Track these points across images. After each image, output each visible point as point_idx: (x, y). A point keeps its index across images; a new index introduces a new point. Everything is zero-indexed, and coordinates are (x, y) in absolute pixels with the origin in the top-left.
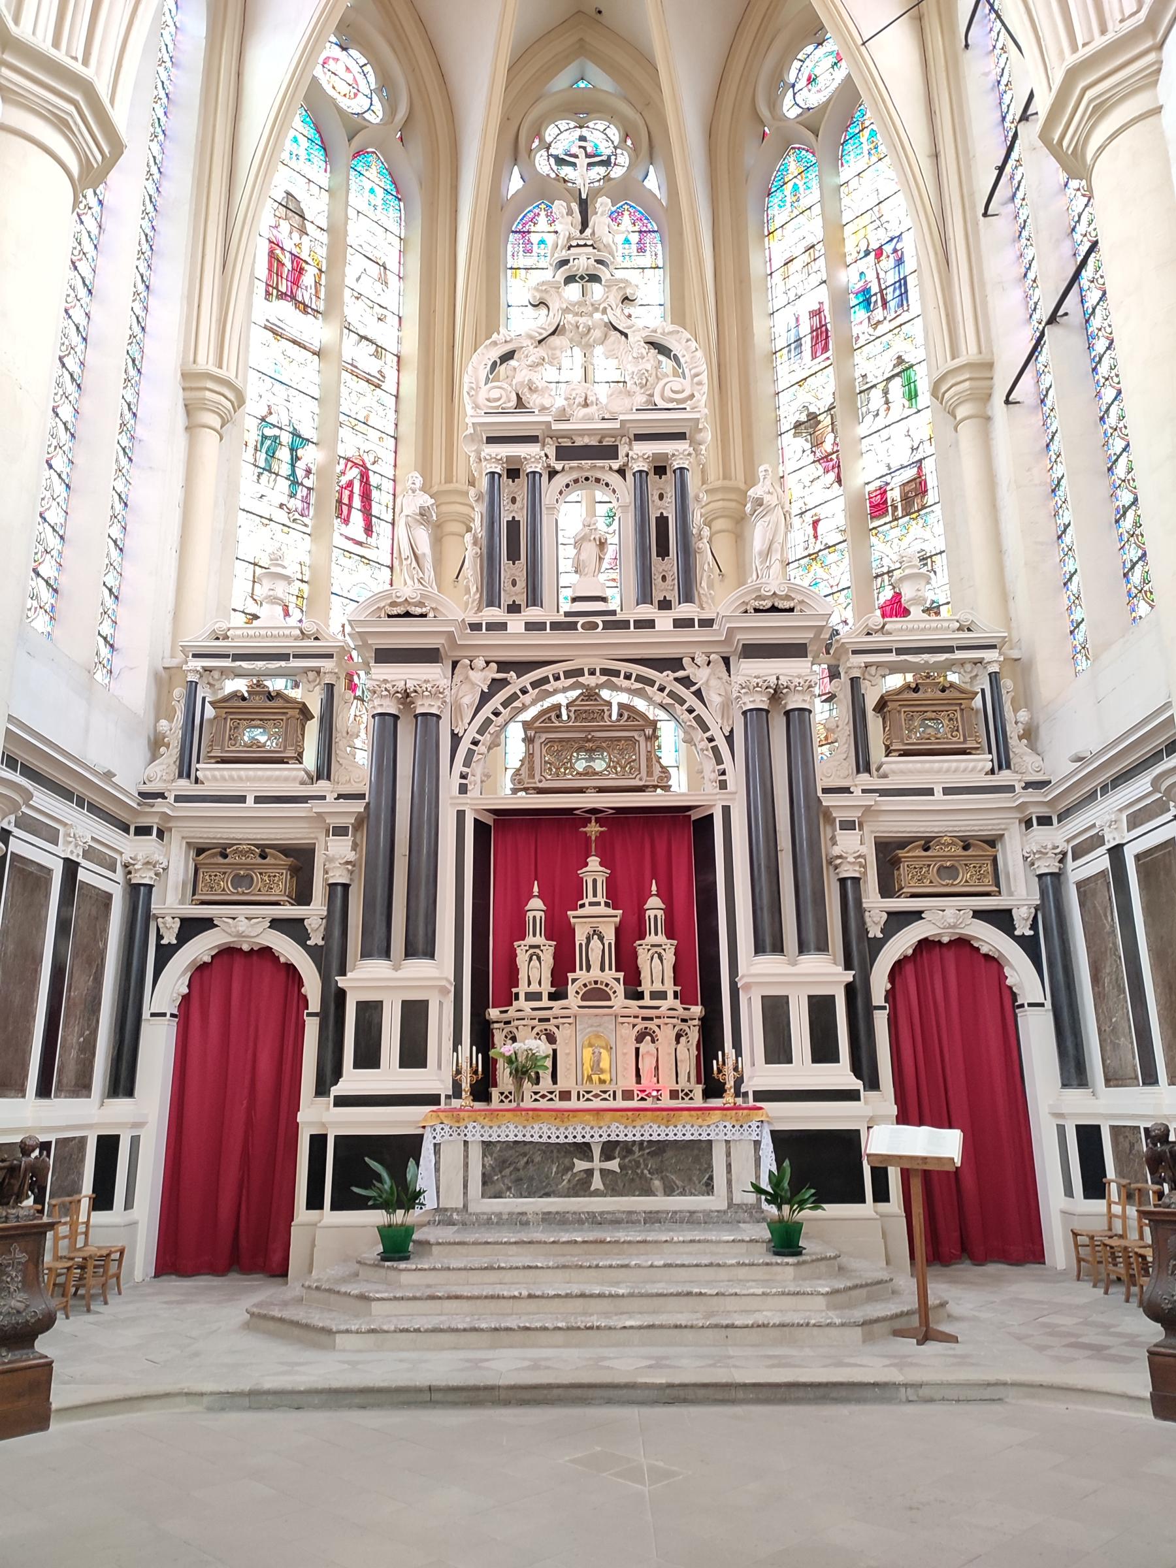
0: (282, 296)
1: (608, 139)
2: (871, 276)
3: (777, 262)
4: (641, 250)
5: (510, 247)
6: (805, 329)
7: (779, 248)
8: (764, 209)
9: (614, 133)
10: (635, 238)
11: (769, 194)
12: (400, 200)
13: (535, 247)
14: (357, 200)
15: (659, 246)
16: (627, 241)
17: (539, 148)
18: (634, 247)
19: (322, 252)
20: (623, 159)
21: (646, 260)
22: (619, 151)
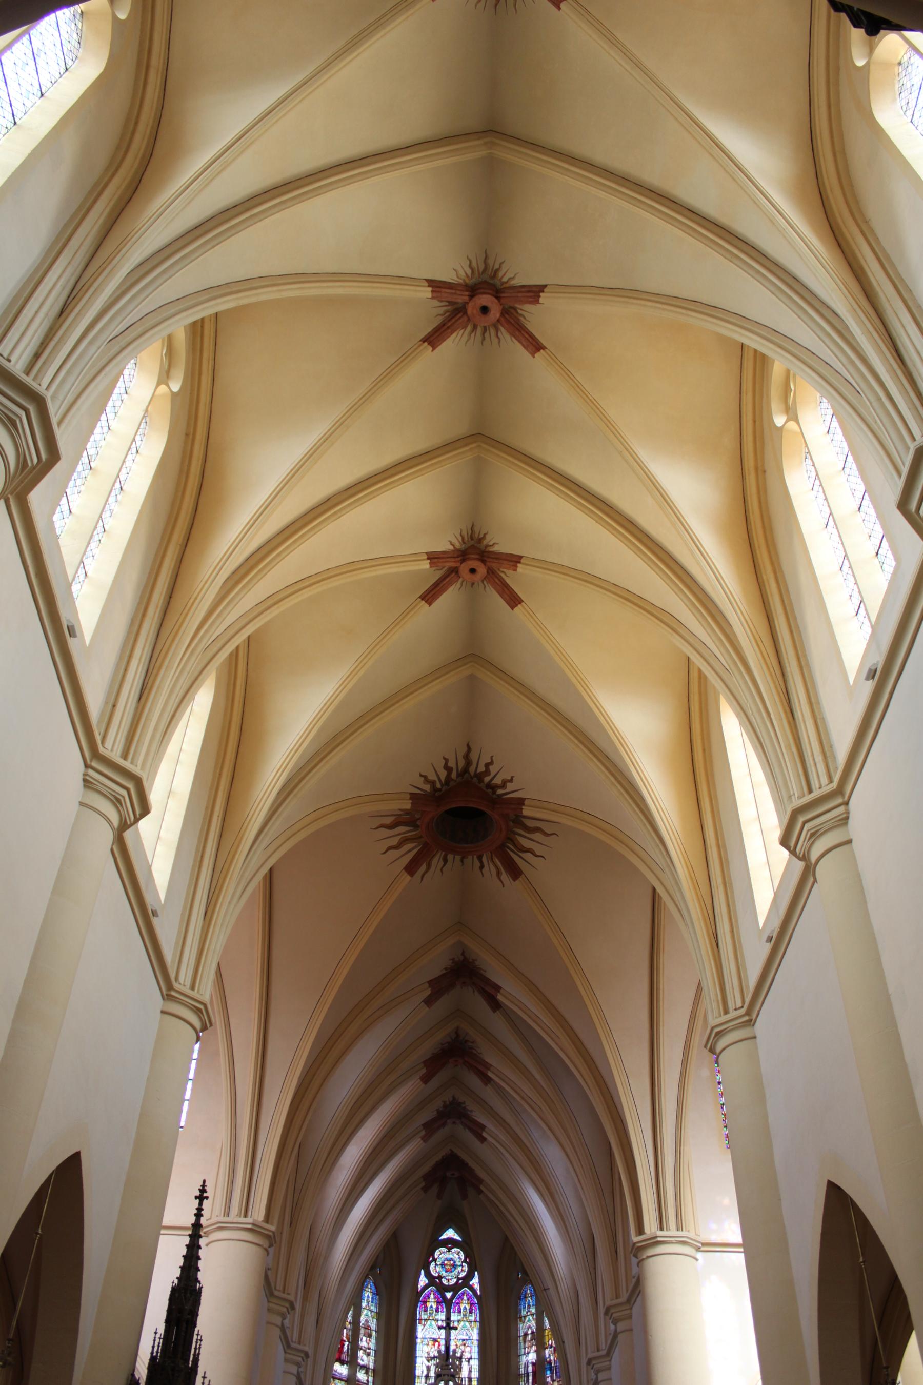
0: (337, 1361)
1: (460, 1258)
2: (552, 1358)
3: (522, 1334)
4: (471, 1312)
5: (418, 1309)
6: (530, 1369)
7: (523, 1328)
8: (517, 1305)
9: (462, 1256)
10: (468, 1307)
11: (520, 1299)
12: (377, 1295)
13: (428, 1309)
14: (364, 1304)
15: (478, 1311)
16: (465, 1308)
17: (432, 1262)
18: (468, 1311)
19: (350, 1333)
20: (466, 1268)
21: (472, 1318)
22: (464, 1264)
